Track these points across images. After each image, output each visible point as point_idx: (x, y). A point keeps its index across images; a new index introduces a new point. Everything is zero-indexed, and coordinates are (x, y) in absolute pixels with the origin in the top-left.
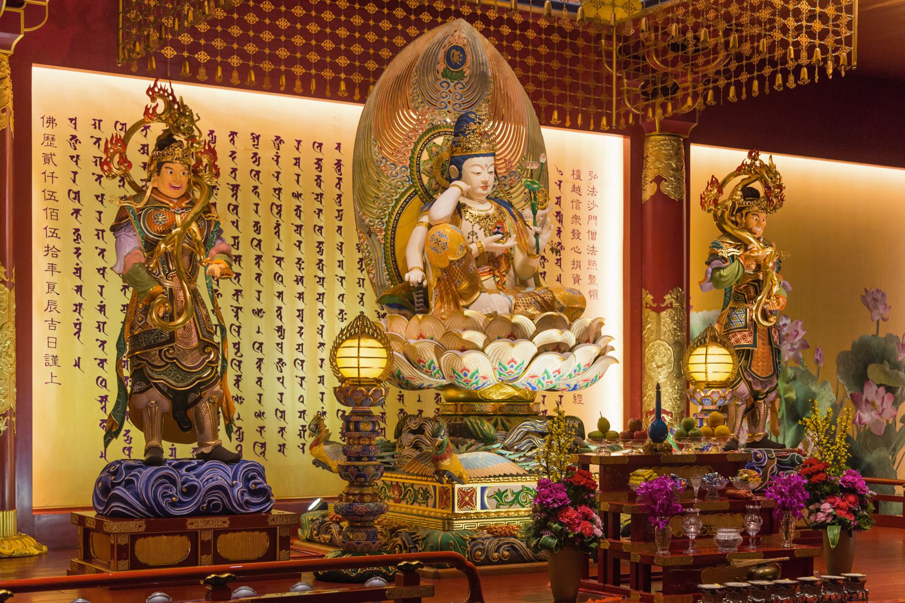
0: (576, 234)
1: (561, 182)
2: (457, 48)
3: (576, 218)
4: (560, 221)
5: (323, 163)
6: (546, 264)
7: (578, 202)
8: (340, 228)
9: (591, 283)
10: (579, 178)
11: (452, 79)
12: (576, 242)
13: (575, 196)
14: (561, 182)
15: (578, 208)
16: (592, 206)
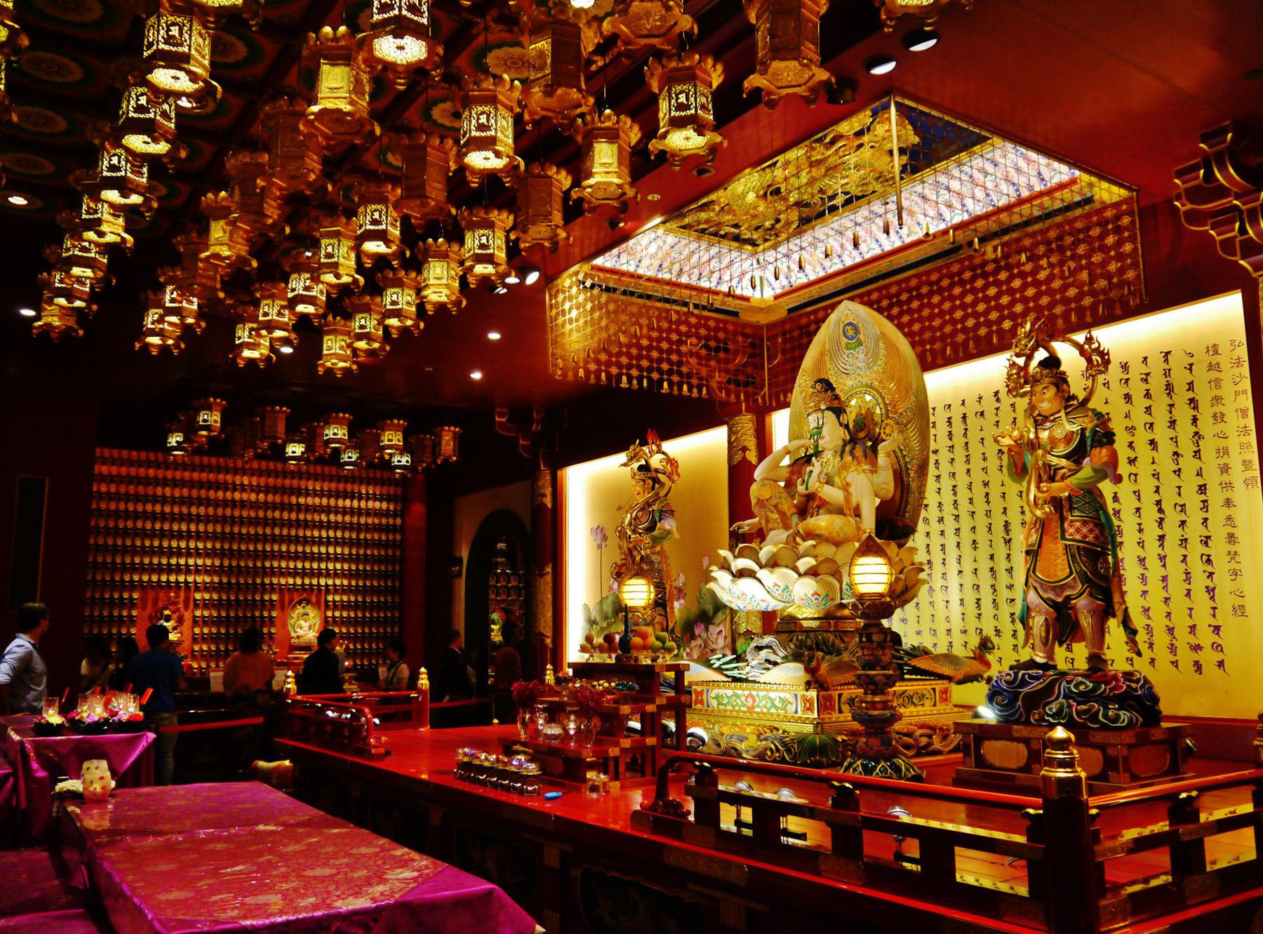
0: (1219, 418)
1: (1191, 365)
2: (849, 324)
3: (1217, 399)
4: (1196, 408)
5: (953, 420)
6: (1180, 460)
7: (1218, 381)
8: (968, 470)
9: (1246, 470)
10: (1216, 352)
11: (854, 349)
12: (1220, 426)
13: (1214, 374)
14: (1191, 365)
15: (1218, 386)
16: (1238, 380)
